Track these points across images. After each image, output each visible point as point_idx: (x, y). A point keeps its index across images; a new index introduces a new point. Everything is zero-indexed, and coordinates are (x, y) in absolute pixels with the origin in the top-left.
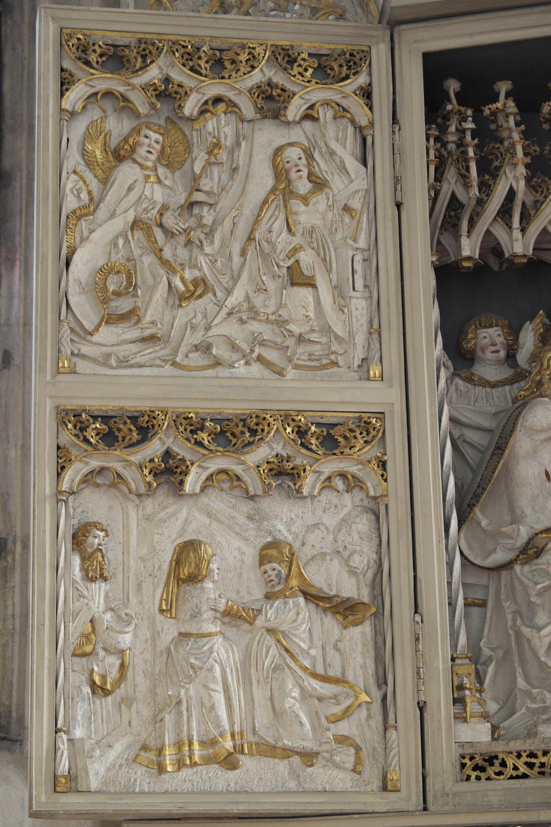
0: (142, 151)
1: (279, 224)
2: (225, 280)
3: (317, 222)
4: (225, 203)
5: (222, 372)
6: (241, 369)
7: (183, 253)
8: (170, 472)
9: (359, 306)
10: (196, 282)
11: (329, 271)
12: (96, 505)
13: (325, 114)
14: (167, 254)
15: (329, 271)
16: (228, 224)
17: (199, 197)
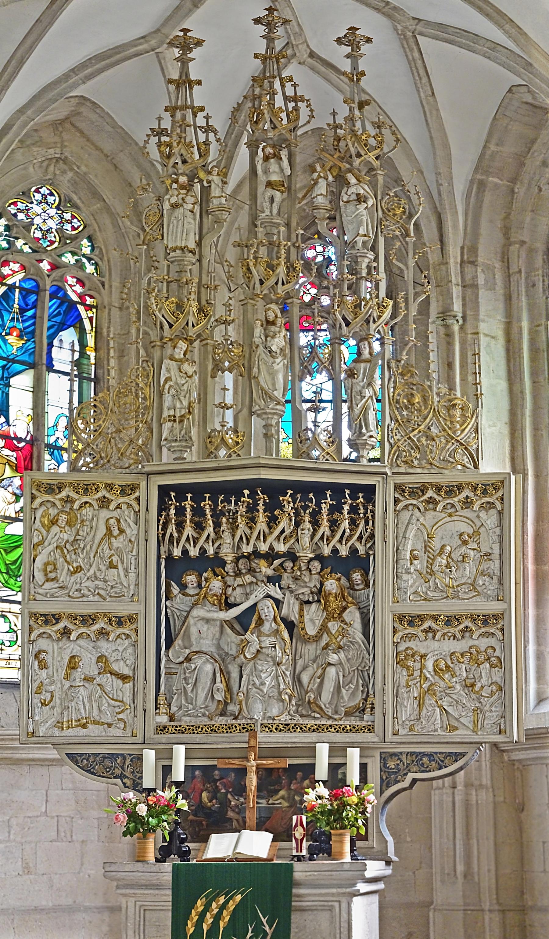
0: (60, 521)
1: (106, 546)
2: (88, 567)
3: (121, 546)
4: (89, 539)
5: (85, 599)
6: (91, 598)
7: (74, 557)
8: (66, 632)
9: (132, 576)
10: (77, 568)
11: (123, 563)
12: (43, 644)
13: (124, 507)
14: (68, 557)
15: (123, 563)
16: (88, 547)
17: (78, 537)
